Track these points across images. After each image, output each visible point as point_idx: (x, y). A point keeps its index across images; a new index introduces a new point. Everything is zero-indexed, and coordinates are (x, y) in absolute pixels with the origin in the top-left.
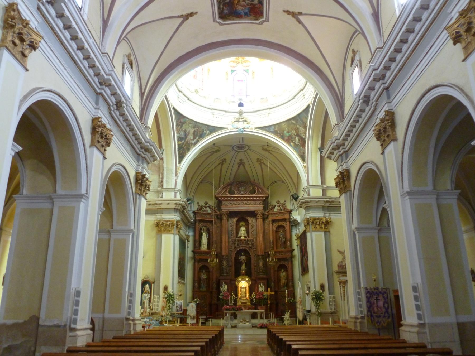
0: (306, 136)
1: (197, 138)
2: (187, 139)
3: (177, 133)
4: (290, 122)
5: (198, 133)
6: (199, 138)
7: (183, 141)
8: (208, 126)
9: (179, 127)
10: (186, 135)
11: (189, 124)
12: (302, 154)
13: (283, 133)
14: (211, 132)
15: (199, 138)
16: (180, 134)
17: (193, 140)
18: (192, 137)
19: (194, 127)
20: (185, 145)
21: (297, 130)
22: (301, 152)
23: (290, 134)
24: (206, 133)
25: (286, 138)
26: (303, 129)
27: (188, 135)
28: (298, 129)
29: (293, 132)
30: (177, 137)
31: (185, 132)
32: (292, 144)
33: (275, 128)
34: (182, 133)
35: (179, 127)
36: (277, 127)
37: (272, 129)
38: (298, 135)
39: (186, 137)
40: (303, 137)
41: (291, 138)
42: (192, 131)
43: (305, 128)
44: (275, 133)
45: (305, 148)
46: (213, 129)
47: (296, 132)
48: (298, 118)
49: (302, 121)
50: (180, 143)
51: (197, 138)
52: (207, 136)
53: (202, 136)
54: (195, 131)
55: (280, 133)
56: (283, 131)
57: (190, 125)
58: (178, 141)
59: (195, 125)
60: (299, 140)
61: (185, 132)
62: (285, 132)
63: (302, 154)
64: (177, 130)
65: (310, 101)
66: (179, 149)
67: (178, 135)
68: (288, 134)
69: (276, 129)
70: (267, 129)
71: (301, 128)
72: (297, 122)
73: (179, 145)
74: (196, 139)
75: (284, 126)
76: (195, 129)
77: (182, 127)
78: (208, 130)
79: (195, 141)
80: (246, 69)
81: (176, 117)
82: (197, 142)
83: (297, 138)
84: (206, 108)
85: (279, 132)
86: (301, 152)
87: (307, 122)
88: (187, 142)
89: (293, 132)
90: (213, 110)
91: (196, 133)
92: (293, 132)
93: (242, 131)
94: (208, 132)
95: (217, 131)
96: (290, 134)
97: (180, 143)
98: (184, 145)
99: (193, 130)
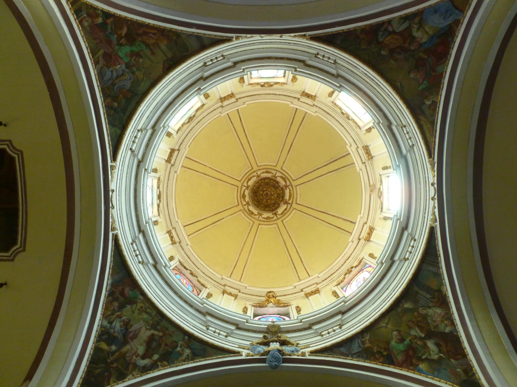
0: (453, 324)
1: (156, 357)
2: (127, 348)
3: (105, 316)
4: (399, 310)
5: (160, 345)
6: (161, 360)
7: (114, 348)
8: (191, 336)
9: (116, 304)
10: (128, 335)
11: (142, 310)
12: (463, 377)
13: (387, 349)
14: (194, 356)
15: (159, 360)
16: (111, 323)
17: (143, 357)
18: (141, 350)
19: (154, 327)
20: (116, 360)
21: (422, 322)
22: (456, 374)
23: (407, 341)
24: (181, 354)
25: (400, 358)
26: (439, 311)
27: (133, 338)
28: (425, 317)
29: (413, 332)
30: (101, 326)
31: (127, 325)
32: (422, 366)
33: (363, 343)
34: (117, 325)
35: (116, 304)
36: (367, 337)
37: (356, 347)
38: (430, 335)
39: (125, 342)
40: (448, 330)
41: (414, 350)
42: (145, 334)
43: (443, 303)
44: (367, 354)
45: (465, 356)
46: (202, 348)
47: (421, 329)
48: (416, 288)
49: (429, 290)
50: (104, 346)
51: (156, 357)
52: (184, 361)
53: (168, 358)
54: (152, 338)
55: (379, 352)
56: (388, 343)
57: (145, 316)
58: (100, 338)
59: (158, 323)
60: (437, 345)
61: (127, 325)
62: (393, 343)
63: (463, 377)
64: (106, 308)
65: (430, 217)
66: (92, 361)
67: (105, 323)
68: (401, 347)
69: (368, 345)
70: (343, 350)
71: (430, 312)
72: (416, 301)
73: (97, 349)
74: (150, 357)
75: (388, 328)
76: (156, 333)
77: (121, 307)
78: (189, 347)
79: (147, 361)
80: (282, 310)
81: (113, 269)
82: (153, 367)
83: (430, 344)
84: (191, 306)
85: (375, 349)
86: (456, 374)
87: (441, 283)
88: (123, 356)
89: (416, 332)
90: (209, 318)
91: (154, 344)
92: (413, 332)
93: (277, 359)
94: (187, 352)
95: (210, 356)
96: (407, 341)
97: (104, 346)
98: (112, 358)
99: (149, 333)
